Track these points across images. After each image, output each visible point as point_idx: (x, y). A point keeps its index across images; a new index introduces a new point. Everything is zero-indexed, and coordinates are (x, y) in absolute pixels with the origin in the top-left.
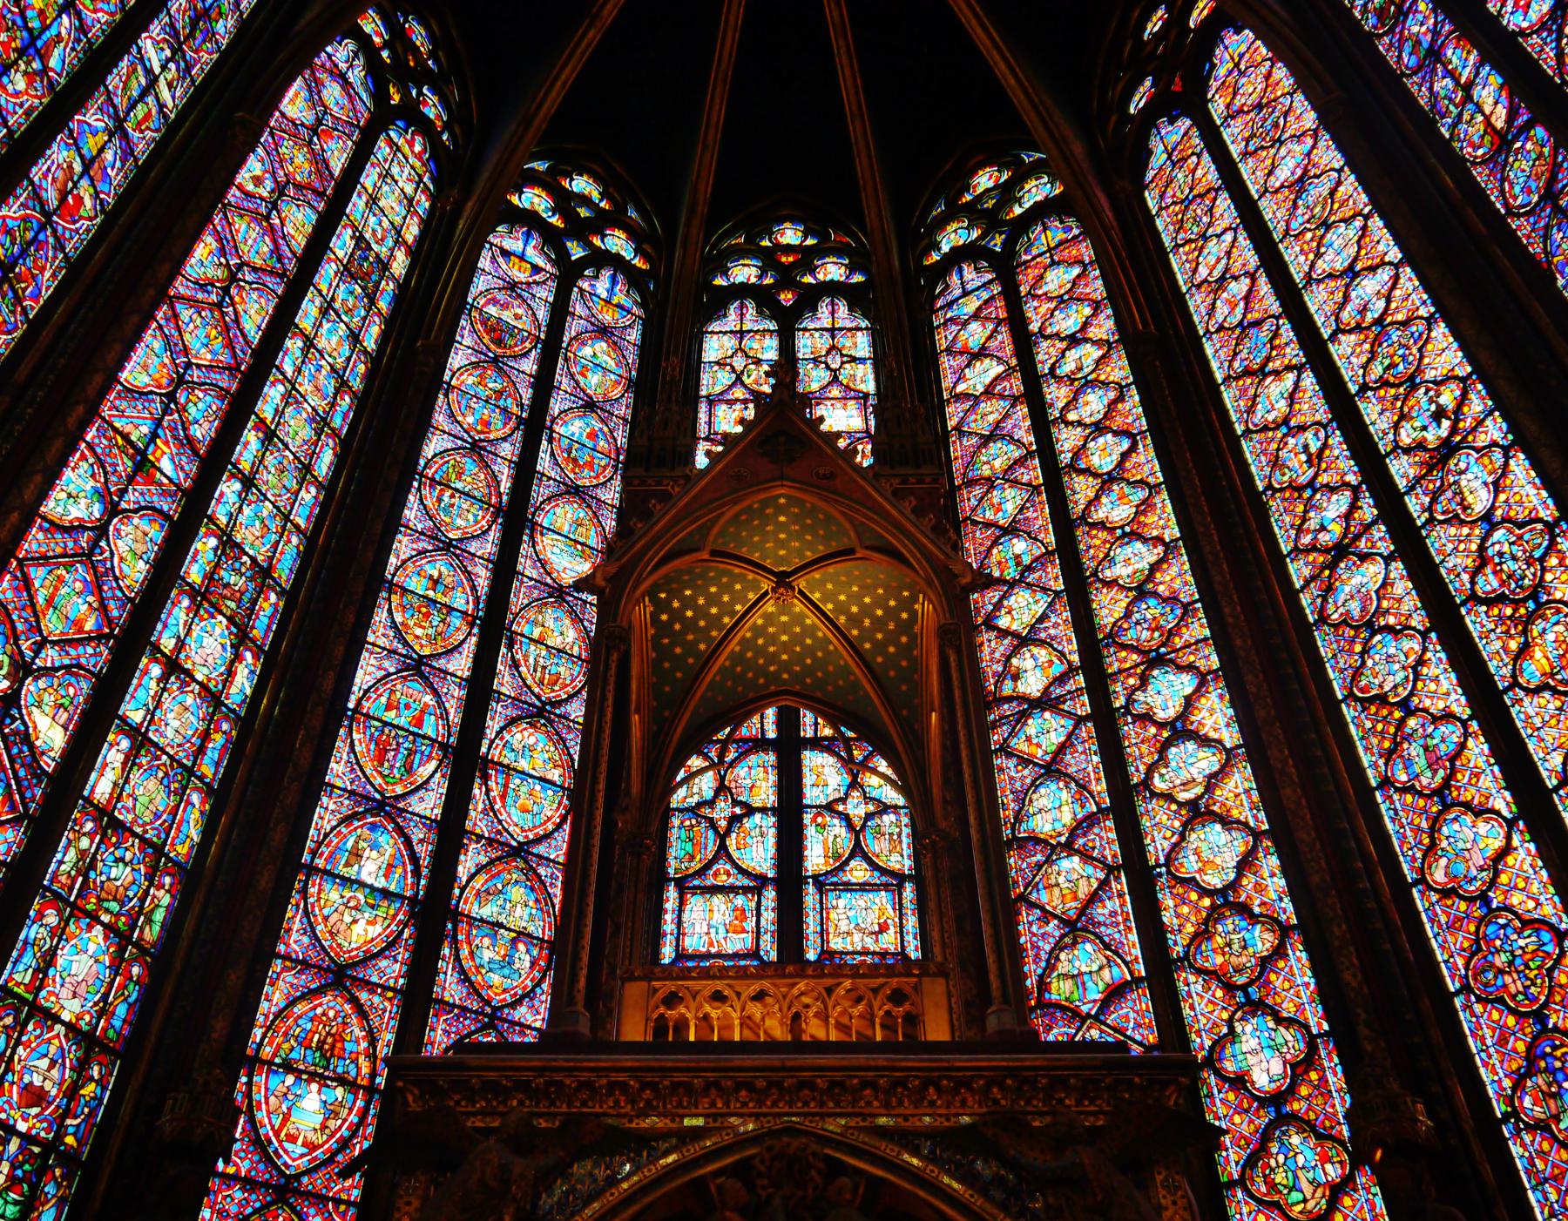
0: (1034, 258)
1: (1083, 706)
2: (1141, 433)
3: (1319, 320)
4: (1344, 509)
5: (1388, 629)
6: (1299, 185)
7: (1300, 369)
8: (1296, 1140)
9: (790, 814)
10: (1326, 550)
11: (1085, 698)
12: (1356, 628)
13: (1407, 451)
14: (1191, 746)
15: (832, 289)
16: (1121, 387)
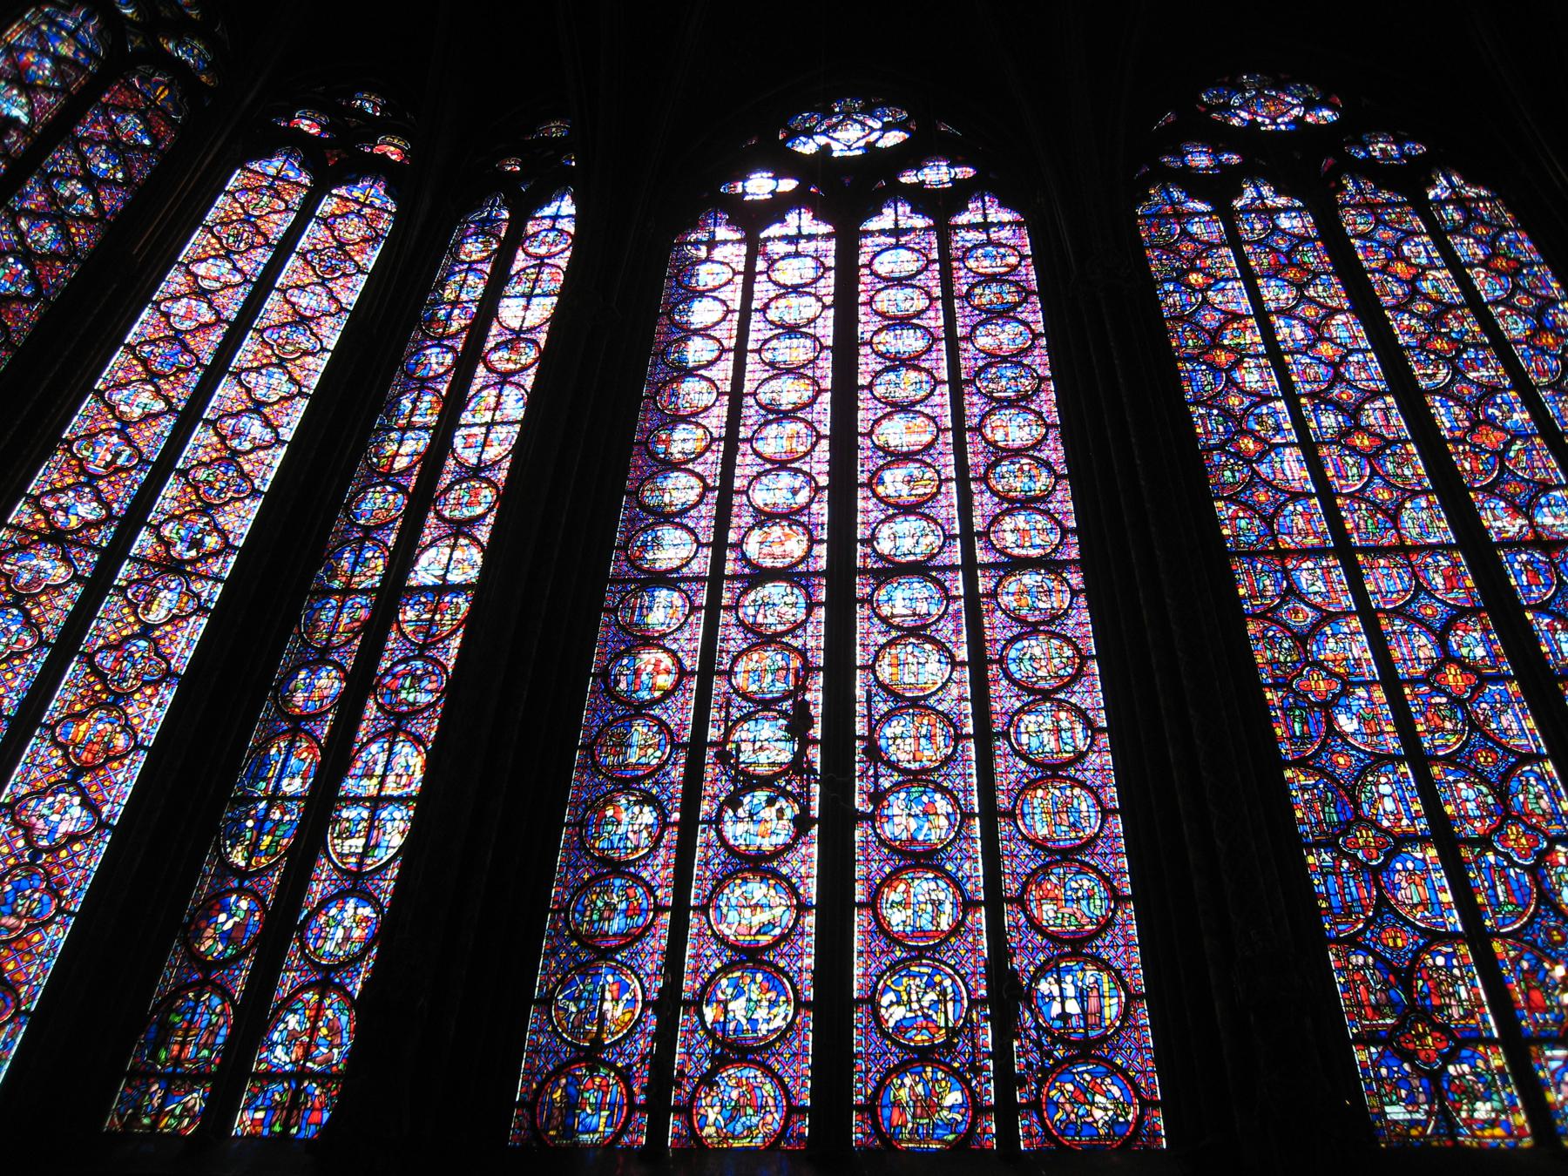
0: (139, 91)
2: (47, 299)
3: (214, 402)
4: (90, 517)
5: (26, 614)
6: (302, 320)
7: (171, 409)
10: (50, 524)
12: (10, 590)
13: (160, 538)
16: (74, 253)
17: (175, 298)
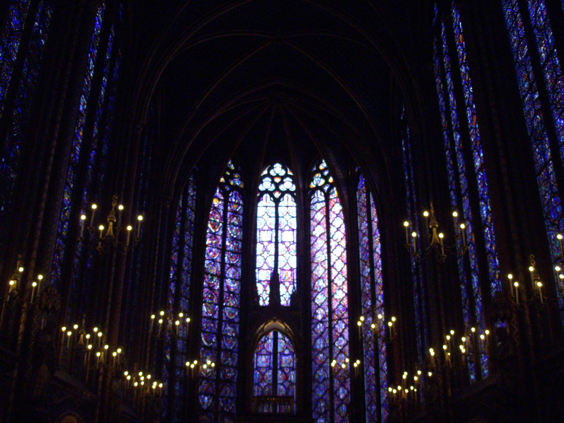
1: (327, 325)
3: (375, 262)
8: (343, 406)
9: (275, 339)
11: (328, 323)
14: (342, 339)
15: (288, 191)
17: (362, 240)
